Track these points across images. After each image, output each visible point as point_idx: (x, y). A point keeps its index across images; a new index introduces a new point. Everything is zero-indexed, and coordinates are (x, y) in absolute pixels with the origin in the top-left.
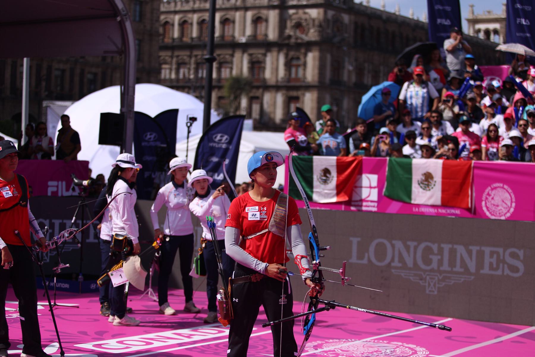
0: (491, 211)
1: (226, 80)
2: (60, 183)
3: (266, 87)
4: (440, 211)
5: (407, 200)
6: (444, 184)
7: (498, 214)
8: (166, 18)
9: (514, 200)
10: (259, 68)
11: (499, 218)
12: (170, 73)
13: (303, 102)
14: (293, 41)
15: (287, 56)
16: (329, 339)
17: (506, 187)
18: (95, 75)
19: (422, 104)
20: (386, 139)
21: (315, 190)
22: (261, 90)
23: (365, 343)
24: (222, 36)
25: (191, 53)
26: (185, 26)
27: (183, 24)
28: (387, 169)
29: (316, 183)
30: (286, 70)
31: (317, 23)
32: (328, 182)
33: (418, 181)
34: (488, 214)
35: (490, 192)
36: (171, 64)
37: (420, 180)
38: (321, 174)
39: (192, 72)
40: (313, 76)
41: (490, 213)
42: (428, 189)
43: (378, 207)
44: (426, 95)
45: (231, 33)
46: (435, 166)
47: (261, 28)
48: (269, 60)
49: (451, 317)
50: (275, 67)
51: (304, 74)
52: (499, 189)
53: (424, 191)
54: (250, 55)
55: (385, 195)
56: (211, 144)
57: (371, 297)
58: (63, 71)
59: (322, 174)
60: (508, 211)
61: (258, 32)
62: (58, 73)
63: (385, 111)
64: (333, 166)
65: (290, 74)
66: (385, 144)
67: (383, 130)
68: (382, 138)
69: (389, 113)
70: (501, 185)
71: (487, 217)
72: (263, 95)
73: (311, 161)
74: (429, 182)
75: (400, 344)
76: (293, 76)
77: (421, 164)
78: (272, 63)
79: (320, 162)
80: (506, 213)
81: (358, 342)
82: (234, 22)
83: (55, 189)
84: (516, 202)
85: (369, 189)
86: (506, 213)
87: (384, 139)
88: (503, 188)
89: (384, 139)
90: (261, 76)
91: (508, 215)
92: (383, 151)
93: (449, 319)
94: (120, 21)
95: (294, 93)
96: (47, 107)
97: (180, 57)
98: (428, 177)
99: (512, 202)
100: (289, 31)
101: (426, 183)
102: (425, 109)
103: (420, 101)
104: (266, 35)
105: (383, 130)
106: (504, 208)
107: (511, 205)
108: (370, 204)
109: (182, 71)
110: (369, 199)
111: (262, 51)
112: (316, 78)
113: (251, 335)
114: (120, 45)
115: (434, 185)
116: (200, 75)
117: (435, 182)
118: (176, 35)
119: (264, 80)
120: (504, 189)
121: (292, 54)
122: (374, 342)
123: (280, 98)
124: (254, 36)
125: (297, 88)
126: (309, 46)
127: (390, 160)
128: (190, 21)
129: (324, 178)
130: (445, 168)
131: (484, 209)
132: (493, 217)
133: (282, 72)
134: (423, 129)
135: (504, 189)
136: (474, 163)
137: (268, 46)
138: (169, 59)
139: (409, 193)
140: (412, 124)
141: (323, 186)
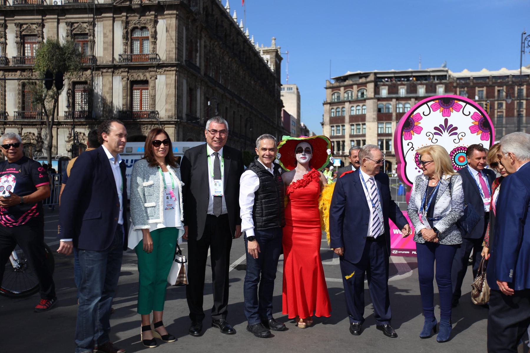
10: (85, 43)
13: (154, 87)
22: (89, 72)
30: (126, 44)
40: (168, 52)
48: (101, 30)
51: (154, 49)
65: (132, 50)
72: (92, 80)
76: (137, 51)
78: (105, 35)
95: (140, 76)
111: (88, 17)
112: (173, 55)
119: (94, 59)
121: (134, 19)
125: (145, 68)
133: (119, 48)
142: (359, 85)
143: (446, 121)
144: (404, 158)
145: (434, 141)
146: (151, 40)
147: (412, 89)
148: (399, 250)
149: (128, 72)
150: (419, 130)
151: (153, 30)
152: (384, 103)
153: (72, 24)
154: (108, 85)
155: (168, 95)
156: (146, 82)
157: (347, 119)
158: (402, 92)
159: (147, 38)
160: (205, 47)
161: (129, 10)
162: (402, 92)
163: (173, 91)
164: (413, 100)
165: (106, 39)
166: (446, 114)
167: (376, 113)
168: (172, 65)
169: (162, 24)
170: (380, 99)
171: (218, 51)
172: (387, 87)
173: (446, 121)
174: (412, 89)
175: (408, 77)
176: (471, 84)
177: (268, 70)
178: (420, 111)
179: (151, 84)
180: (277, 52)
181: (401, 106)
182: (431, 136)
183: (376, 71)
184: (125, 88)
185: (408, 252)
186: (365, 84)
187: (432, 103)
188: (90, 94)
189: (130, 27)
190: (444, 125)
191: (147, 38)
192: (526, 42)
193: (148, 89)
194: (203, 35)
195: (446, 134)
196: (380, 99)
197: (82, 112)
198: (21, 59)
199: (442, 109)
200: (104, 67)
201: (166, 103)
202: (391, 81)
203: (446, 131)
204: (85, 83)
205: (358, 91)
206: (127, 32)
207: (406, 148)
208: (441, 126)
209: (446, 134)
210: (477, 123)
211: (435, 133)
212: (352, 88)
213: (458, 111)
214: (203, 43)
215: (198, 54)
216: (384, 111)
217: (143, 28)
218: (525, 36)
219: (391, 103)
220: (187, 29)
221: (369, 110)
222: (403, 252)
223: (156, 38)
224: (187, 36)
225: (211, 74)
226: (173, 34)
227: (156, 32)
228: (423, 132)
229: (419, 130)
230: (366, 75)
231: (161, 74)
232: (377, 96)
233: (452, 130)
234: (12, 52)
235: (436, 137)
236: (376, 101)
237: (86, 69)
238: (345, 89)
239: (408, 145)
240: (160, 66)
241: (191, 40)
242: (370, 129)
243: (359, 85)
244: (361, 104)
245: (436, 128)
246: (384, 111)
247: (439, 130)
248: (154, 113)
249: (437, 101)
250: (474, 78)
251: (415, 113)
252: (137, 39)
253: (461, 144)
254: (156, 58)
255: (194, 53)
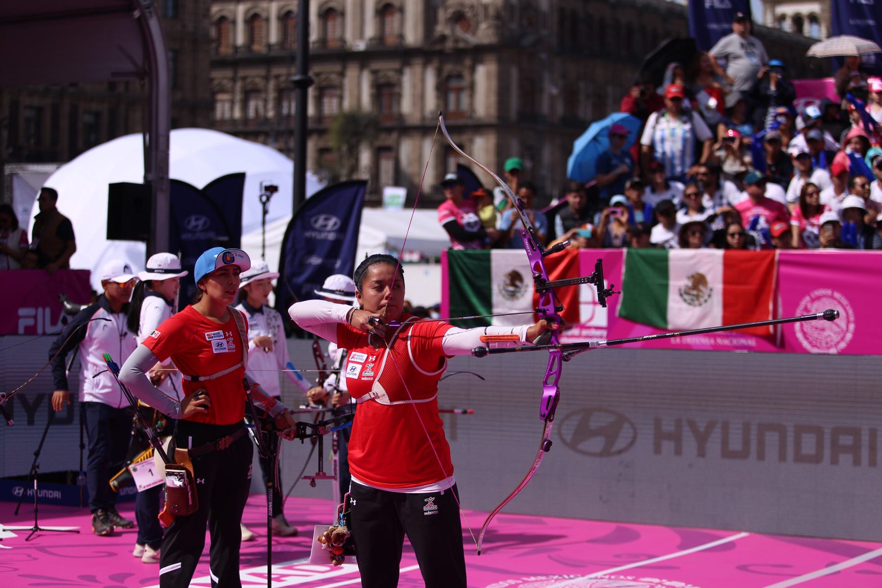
0: (811, 339)
1: (333, 118)
2: (40, 310)
3: (405, 129)
4: (720, 341)
5: (661, 324)
6: (726, 293)
7: (824, 345)
8: (221, 10)
9: (852, 318)
10: (391, 95)
11: (826, 351)
12: (232, 109)
14: (449, 45)
15: (439, 72)
16: (529, 575)
17: (837, 295)
18: (97, 115)
19: (683, 152)
20: (622, 214)
21: (495, 310)
22: (394, 136)
23: (594, 581)
24: (323, 40)
25: (269, 71)
26: (256, 24)
27: (252, 20)
28: (624, 270)
29: (497, 297)
30: (438, 97)
31: (491, 11)
32: (519, 295)
33: (680, 290)
34: (805, 344)
35: (809, 306)
36: (232, 91)
37: (683, 288)
38: (505, 282)
39: (271, 105)
41: (810, 343)
42: (696, 303)
43: (608, 337)
44: (688, 135)
45: (338, 34)
46: (710, 261)
47: (393, 23)
48: (408, 81)
49: (746, 531)
50: (418, 93)
52: (824, 300)
53: (691, 307)
54: (374, 72)
55: (621, 316)
56: (308, 234)
57: (601, 498)
58: (40, 110)
59: (508, 282)
60: (843, 339)
61: (388, 30)
62: (29, 113)
63: (616, 166)
64: (525, 267)
65: (446, 104)
66: (620, 223)
67: (617, 198)
68: (614, 213)
69: (623, 168)
70: (829, 292)
71: (805, 351)
72: (398, 144)
73: (488, 259)
74: (699, 291)
75: (656, 580)
76: (452, 107)
77: (683, 260)
78: (414, 86)
79: (504, 261)
80: (838, 343)
81: (580, 580)
82: (343, 14)
83: (31, 322)
84: (856, 322)
85: (591, 307)
86: (838, 343)
87: (618, 216)
88: (832, 297)
89: (618, 216)
90: (395, 109)
91: (843, 345)
92: (616, 237)
93: (743, 535)
94: (139, 19)
96: (12, 175)
97: (249, 80)
98: (699, 281)
99: (848, 322)
100: (441, 28)
101: (695, 292)
102: (688, 160)
103: (678, 146)
104: (401, 36)
105: (617, 198)
106: (835, 333)
107: (847, 327)
108: (593, 332)
109: (252, 104)
110: (593, 323)
111: (396, 65)
112: (493, 111)
113: (193, 581)
114: (139, 60)
115: (709, 296)
116: (285, 111)
117: (711, 290)
118: (240, 39)
119: (401, 117)
120: (835, 299)
121: (448, 68)
122: (610, 578)
123: (429, 149)
124: (380, 38)
126: (478, 53)
127: (628, 253)
128: (264, 15)
129: (511, 289)
130: (728, 264)
131: (799, 335)
132: (815, 350)
133: (431, 102)
134: (688, 196)
135: (835, 299)
136: (780, 254)
137: (405, 55)
138: (228, 84)
139: (662, 311)
140: (667, 187)
141: (509, 303)
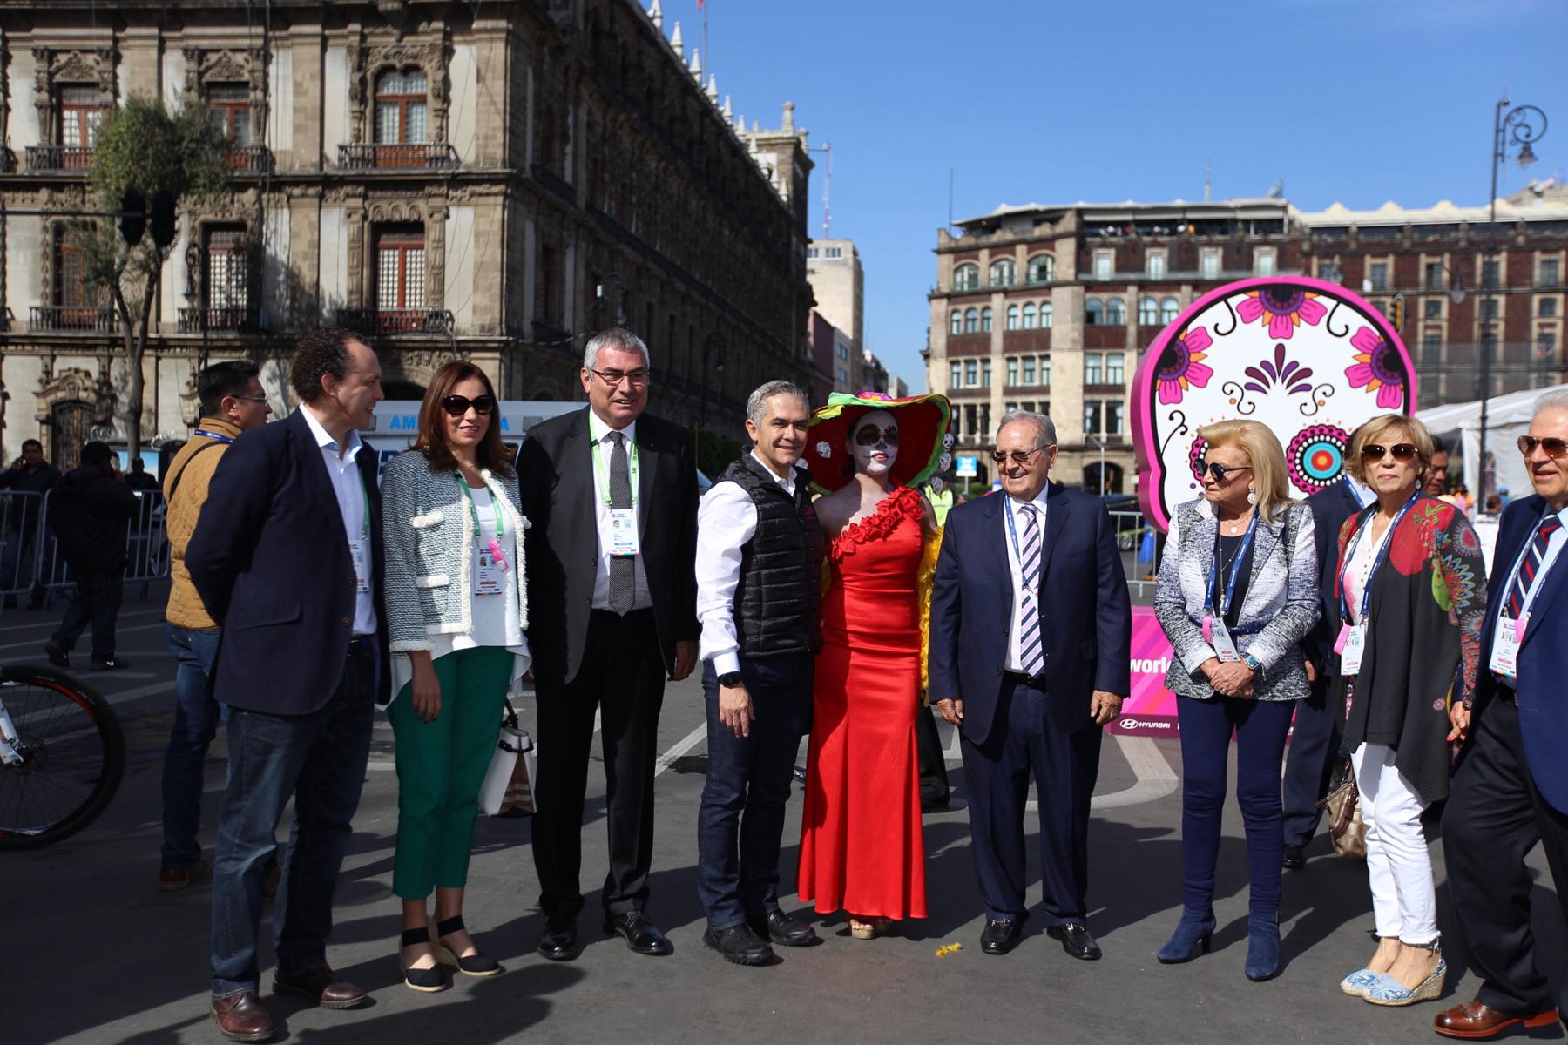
3: (276, 183)
10: (240, 111)
13: (441, 242)
22: (251, 194)
30: (360, 116)
40: (483, 139)
48: (286, 72)
51: (442, 132)
72: (260, 219)
76: (390, 137)
78: (298, 89)
95: (399, 208)
111: (248, 35)
112: (497, 150)
119: (266, 157)
121: (385, 42)
125: (415, 185)
133: (340, 126)
142: (1033, 244)
143: (1280, 351)
144: (1159, 456)
145: (1245, 407)
146: (433, 103)
147: (1185, 258)
148: (1140, 718)
149: (365, 197)
150: (1202, 377)
151: (440, 75)
152: (1104, 296)
153: (203, 53)
154: (307, 236)
155: (479, 267)
156: (416, 227)
157: (997, 342)
158: (1157, 265)
159: (421, 100)
160: (590, 126)
161: (370, 16)
162: (1157, 265)
163: (494, 253)
164: (1186, 289)
165: (303, 101)
166: (1281, 330)
167: (1079, 326)
168: (493, 180)
169: (465, 58)
170: (1091, 286)
171: (626, 141)
172: (1112, 252)
173: (1280, 351)
174: (1185, 258)
175: (1172, 224)
176: (1353, 246)
177: (772, 195)
178: (1205, 320)
179: (432, 234)
180: (797, 144)
181: (1151, 305)
182: (1237, 395)
183: (1081, 204)
184: (355, 244)
185: (1167, 725)
186: (1049, 242)
187: (1242, 298)
188: (254, 259)
189: (373, 66)
190: (1273, 361)
191: (421, 100)
192: (1509, 129)
193: (421, 247)
194: (585, 92)
195: (1278, 388)
196: (1091, 286)
197: (230, 311)
198: (53, 154)
199: (1268, 315)
200: (296, 181)
201: (476, 288)
202: (1125, 233)
203: (1279, 380)
204: (239, 226)
205: (1029, 262)
206: (363, 81)
207: (1164, 427)
208: (1265, 364)
209: (1278, 388)
210: (1367, 358)
211: (1249, 387)
212: (1013, 253)
213: (1315, 323)
214: (583, 117)
215: (569, 149)
216: (1103, 319)
217: (411, 70)
218: (1505, 111)
219: (1124, 296)
220: (538, 77)
221: (1060, 315)
222: (1154, 725)
223: (446, 100)
224: (537, 97)
225: (608, 207)
226: (498, 87)
227: (446, 82)
228: (1215, 383)
229: (1202, 377)
230: (1053, 216)
231: (460, 203)
232: (1084, 277)
233: (1298, 377)
234: (24, 133)
235: (1251, 395)
236: (1080, 290)
237: (242, 187)
238: (991, 256)
239: (1171, 418)
240: (459, 181)
241: (550, 110)
242: (1062, 371)
243: (1033, 244)
244: (1038, 300)
245: (1250, 372)
246: (1103, 319)
247: (1258, 377)
248: (440, 317)
249: (1256, 294)
250: (1360, 229)
251: (1192, 327)
252: (393, 101)
253: (1321, 418)
254: (446, 158)
255: (557, 143)
